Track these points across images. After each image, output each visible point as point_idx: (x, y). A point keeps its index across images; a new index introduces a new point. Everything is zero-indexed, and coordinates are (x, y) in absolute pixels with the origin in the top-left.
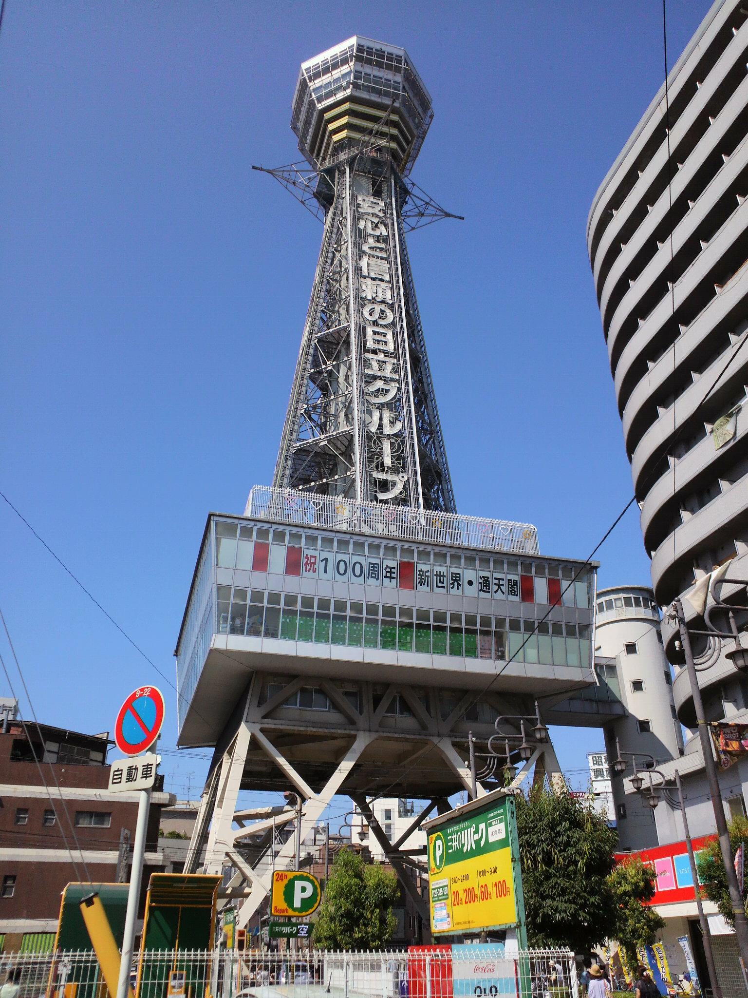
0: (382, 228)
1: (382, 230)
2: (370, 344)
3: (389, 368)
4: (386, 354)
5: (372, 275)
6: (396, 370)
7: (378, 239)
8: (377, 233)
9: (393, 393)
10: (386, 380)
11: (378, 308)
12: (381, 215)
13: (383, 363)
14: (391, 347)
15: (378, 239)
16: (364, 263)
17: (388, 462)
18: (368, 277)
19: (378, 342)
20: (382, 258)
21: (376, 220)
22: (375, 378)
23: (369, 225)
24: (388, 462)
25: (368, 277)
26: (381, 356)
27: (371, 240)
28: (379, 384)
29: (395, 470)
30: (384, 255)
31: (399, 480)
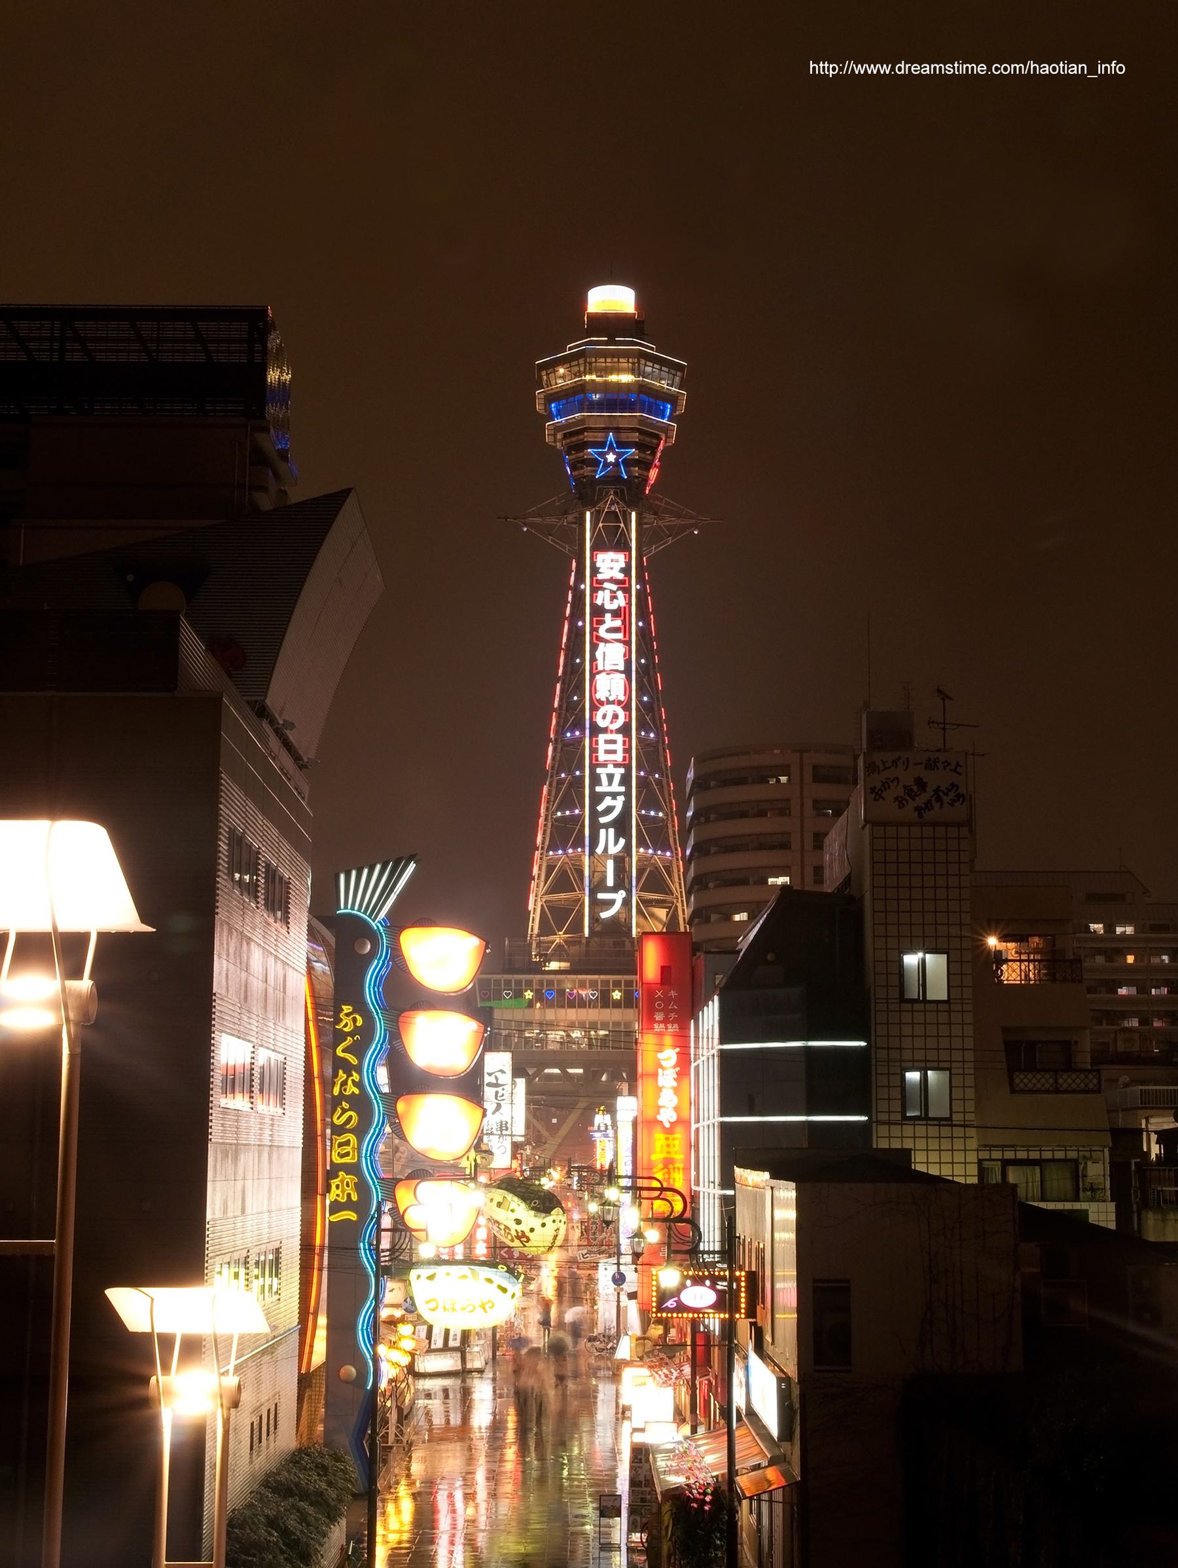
0: (620, 594)
1: (621, 601)
2: (602, 757)
3: (617, 779)
4: (617, 765)
5: (608, 668)
6: (621, 784)
7: (616, 614)
8: (614, 606)
9: (619, 803)
10: (614, 795)
11: (609, 709)
13: (610, 777)
14: (619, 757)
15: (616, 614)
16: (599, 654)
17: (610, 882)
18: (604, 671)
19: (607, 752)
20: (619, 641)
21: (614, 587)
22: (603, 796)
23: (607, 593)
24: (610, 882)
25: (604, 671)
26: (610, 769)
27: (608, 616)
28: (608, 801)
29: (615, 889)
30: (620, 636)
31: (620, 896)
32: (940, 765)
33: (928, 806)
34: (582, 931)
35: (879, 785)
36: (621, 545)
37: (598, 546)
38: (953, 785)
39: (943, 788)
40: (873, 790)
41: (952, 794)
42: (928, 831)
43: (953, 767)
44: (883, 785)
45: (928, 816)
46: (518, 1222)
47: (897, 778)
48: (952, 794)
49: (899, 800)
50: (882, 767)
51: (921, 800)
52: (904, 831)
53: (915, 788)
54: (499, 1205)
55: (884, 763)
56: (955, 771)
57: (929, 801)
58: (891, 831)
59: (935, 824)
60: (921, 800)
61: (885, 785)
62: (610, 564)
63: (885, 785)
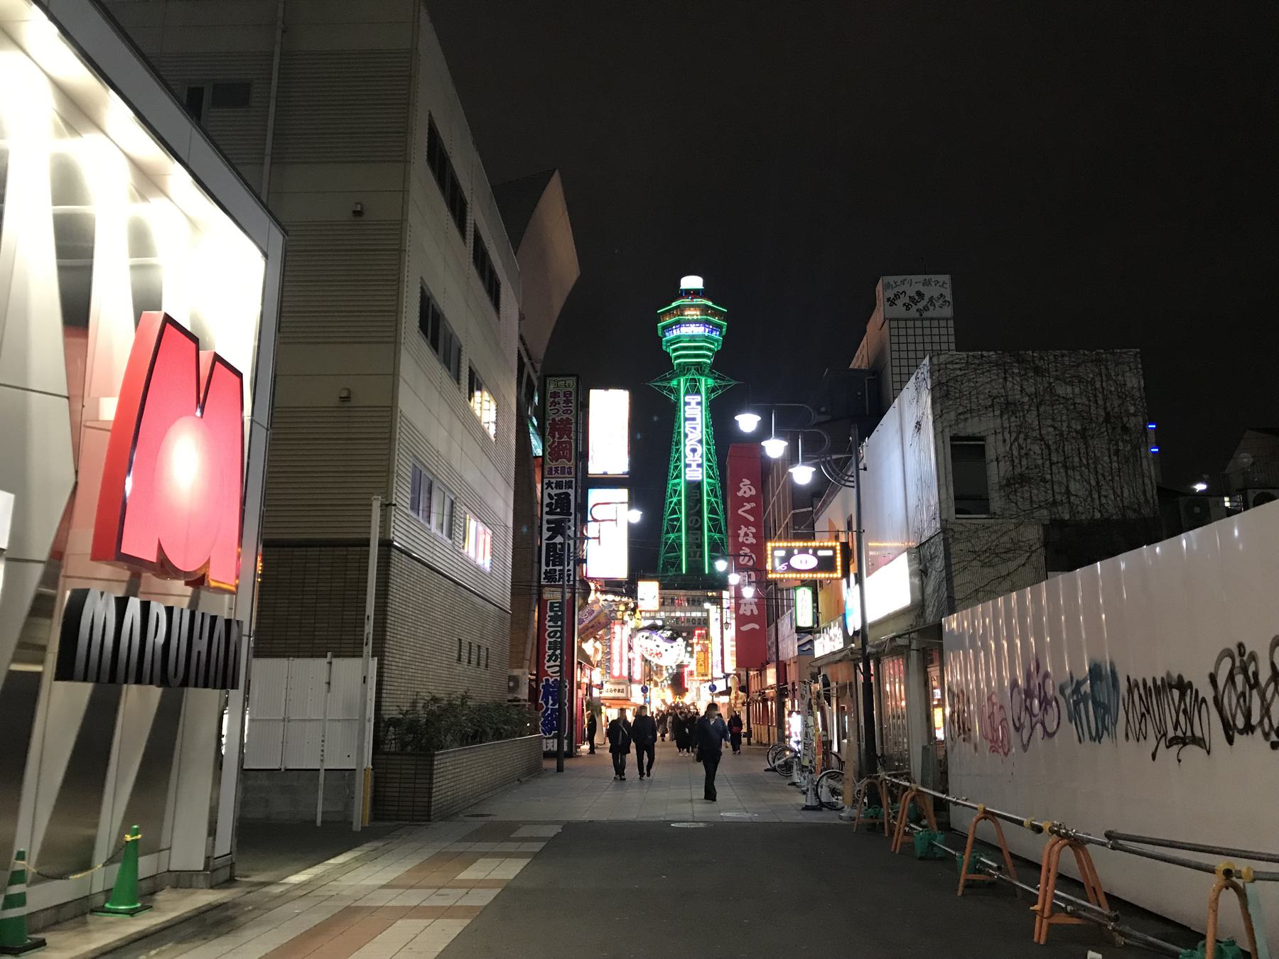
32: (933, 284)
33: (926, 308)
34: (681, 570)
35: (892, 297)
36: (698, 393)
37: (687, 393)
38: (941, 295)
39: (935, 297)
40: (889, 300)
41: (941, 301)
42: (927, 323)
43: (941, 284)
44: (895, 295)
45: (926, 314)
46: (658, 646)
47: (904, 292)
48: (941, 301)
49: (907, 307)
50: (894, 285)
51: (921, 305)
52: (910, 324)
53: (916, 297)
54: (647, 638)
55: (895, 283)
56: (943, 286)
57: (926, 306)
58: (902, 324)
59: (931, 319)
60: (921, 305)
61: (897, 296)
63: (897, 296)
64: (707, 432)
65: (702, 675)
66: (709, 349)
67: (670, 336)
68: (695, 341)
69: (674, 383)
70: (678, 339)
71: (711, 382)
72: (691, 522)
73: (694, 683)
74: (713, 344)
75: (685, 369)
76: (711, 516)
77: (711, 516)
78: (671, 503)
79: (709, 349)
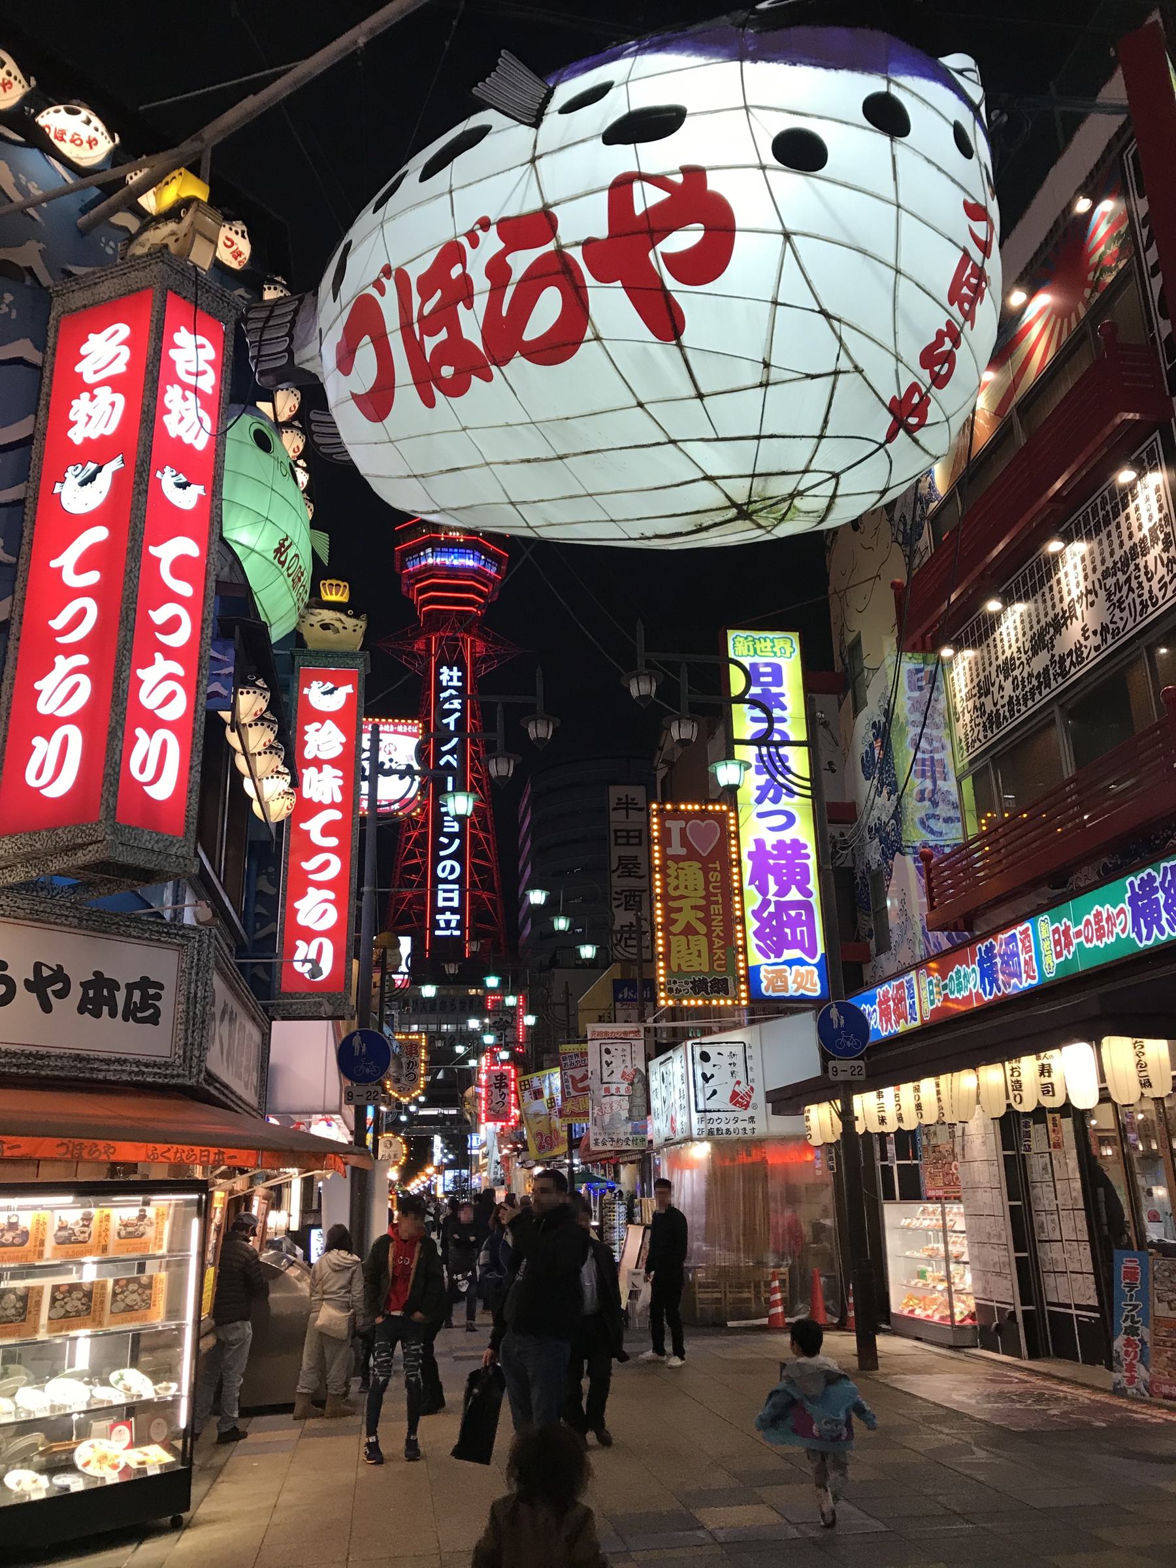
12: (460, 684)
62: (449, 676)
64: (474, 724)
65: (699, 987)
66: (480, 593)
67: (413, 566)
68: (457, 578)
69: (419, 645)
70: (431, 571)
71: (480, 646)
72: (443, 870)
73: (617, 1048)
74: (486, 586)
75: (436, 620)
76: (477, 861)
77: (477, 861)
78: (410, 837)
79: (480, 593)
